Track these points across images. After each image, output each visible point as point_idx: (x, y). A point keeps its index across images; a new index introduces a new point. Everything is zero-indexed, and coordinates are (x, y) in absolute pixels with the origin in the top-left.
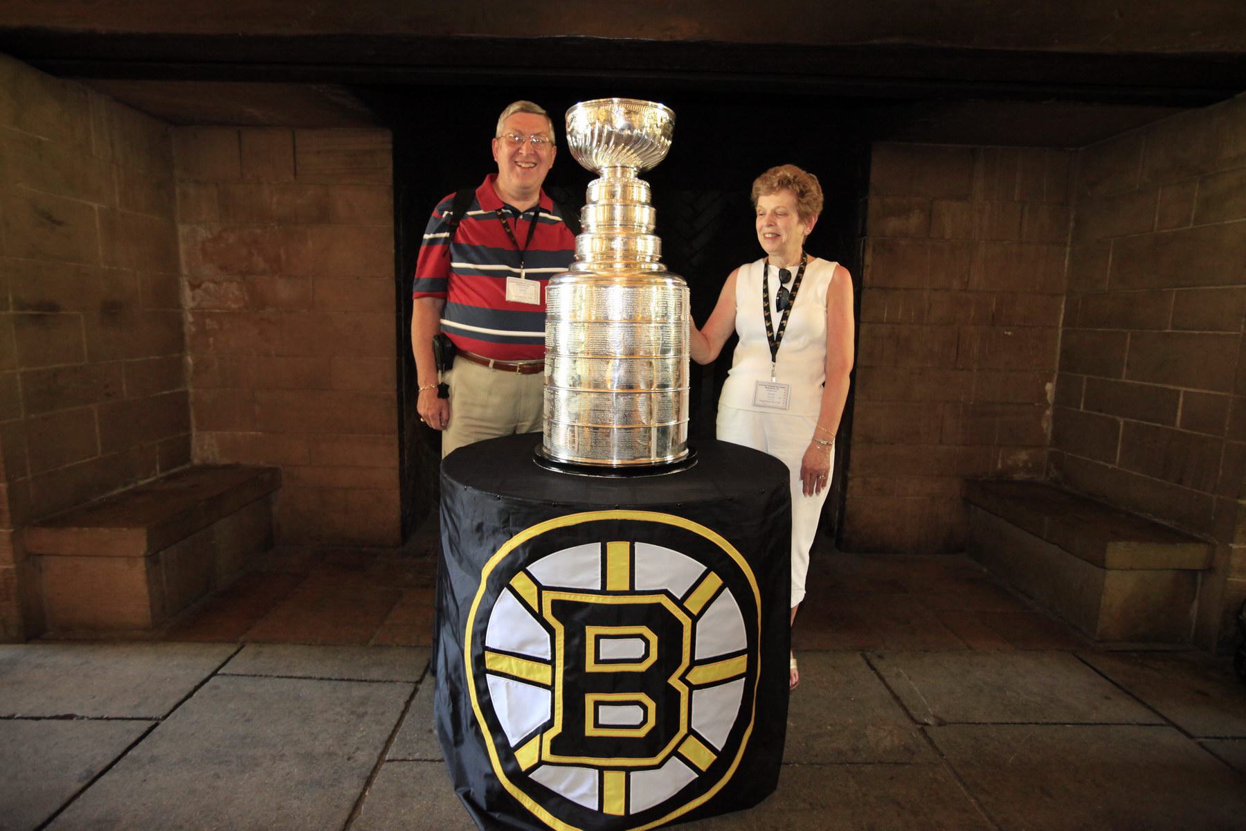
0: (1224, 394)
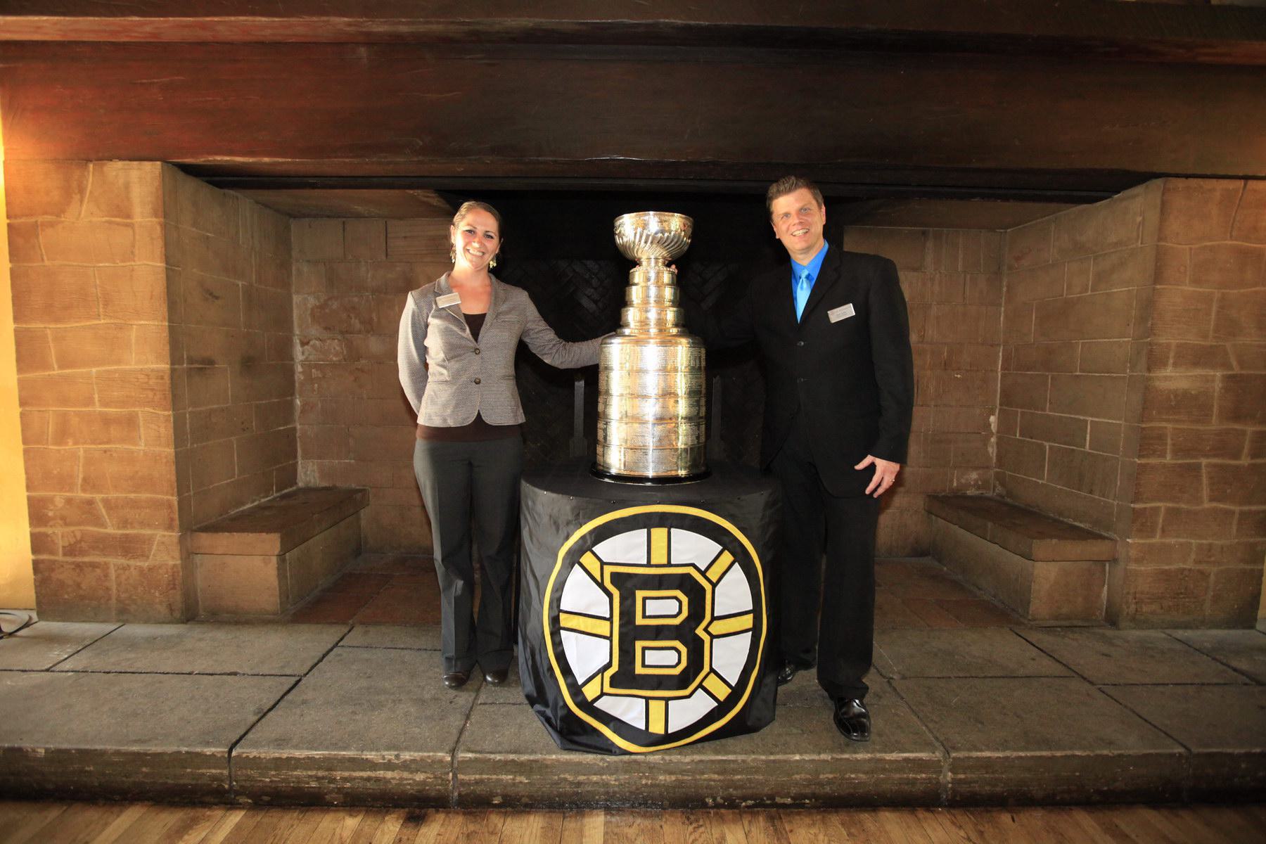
0: (1118, 422)
